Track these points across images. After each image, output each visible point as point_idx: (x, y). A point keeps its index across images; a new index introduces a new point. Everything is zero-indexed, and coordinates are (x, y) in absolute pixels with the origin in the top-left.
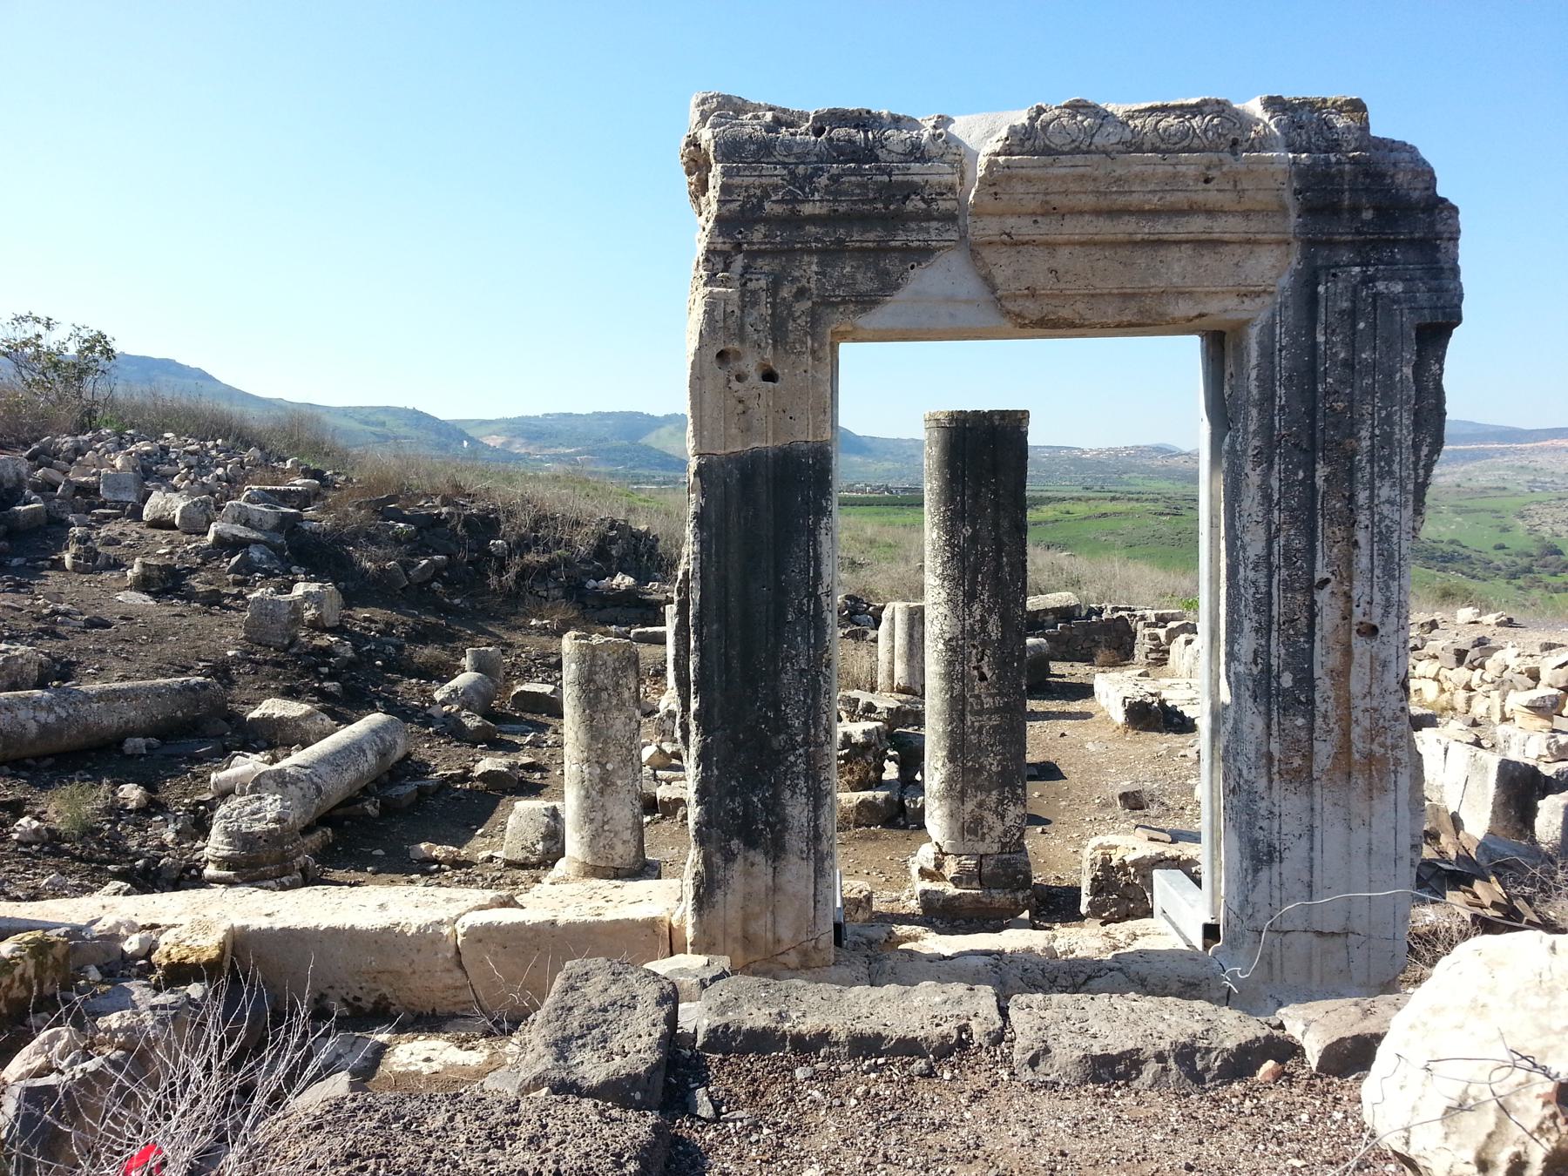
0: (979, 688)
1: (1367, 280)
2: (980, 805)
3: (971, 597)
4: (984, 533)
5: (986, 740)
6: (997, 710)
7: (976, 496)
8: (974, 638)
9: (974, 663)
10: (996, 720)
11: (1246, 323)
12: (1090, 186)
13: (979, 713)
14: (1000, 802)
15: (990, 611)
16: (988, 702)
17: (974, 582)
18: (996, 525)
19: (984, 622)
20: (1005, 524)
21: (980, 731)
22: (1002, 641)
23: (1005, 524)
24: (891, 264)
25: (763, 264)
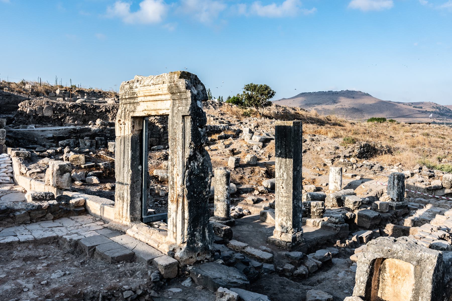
0: (282, 190)
1: (179, 106)
2: (282, 220)
3: (280, 167)
4: (283, 152)
5: (284, 204)
6: (286, 197)
7: (281, 143)
8: (281, 178)
9: (281, 184)
10: (285, 199)
11: (169, 115)
12: (148, 92)
13: (282, 197)
14: (287, 220)
15: (284, 172)
16: (284, 195)
17: (281, 164)
18: (286, 151)
19: (283, 174)
20: (287, 150)
21: (282, 201)
22: (287, 179)
23: (287, 150)
24: (135, 105)
25: (125, 106)
